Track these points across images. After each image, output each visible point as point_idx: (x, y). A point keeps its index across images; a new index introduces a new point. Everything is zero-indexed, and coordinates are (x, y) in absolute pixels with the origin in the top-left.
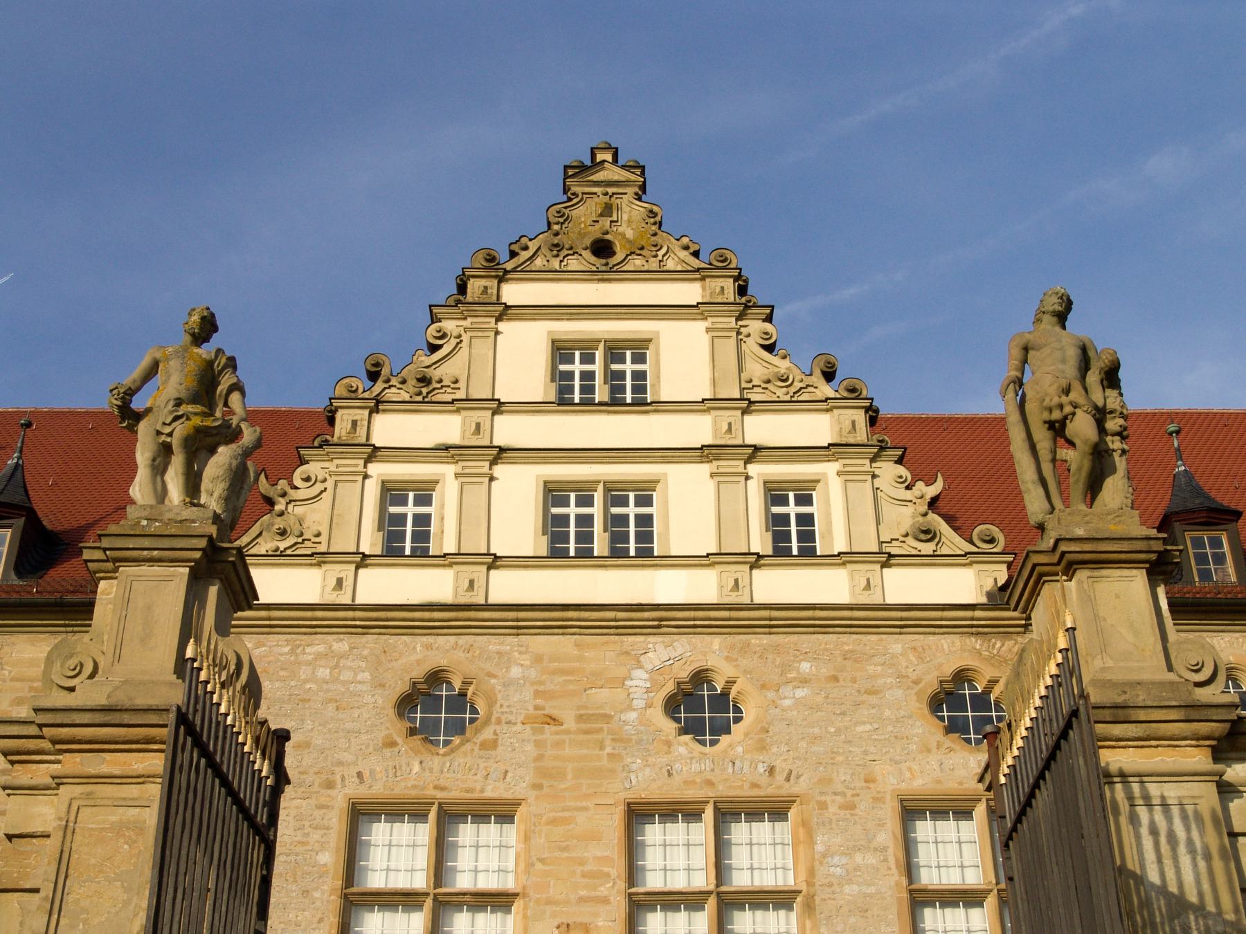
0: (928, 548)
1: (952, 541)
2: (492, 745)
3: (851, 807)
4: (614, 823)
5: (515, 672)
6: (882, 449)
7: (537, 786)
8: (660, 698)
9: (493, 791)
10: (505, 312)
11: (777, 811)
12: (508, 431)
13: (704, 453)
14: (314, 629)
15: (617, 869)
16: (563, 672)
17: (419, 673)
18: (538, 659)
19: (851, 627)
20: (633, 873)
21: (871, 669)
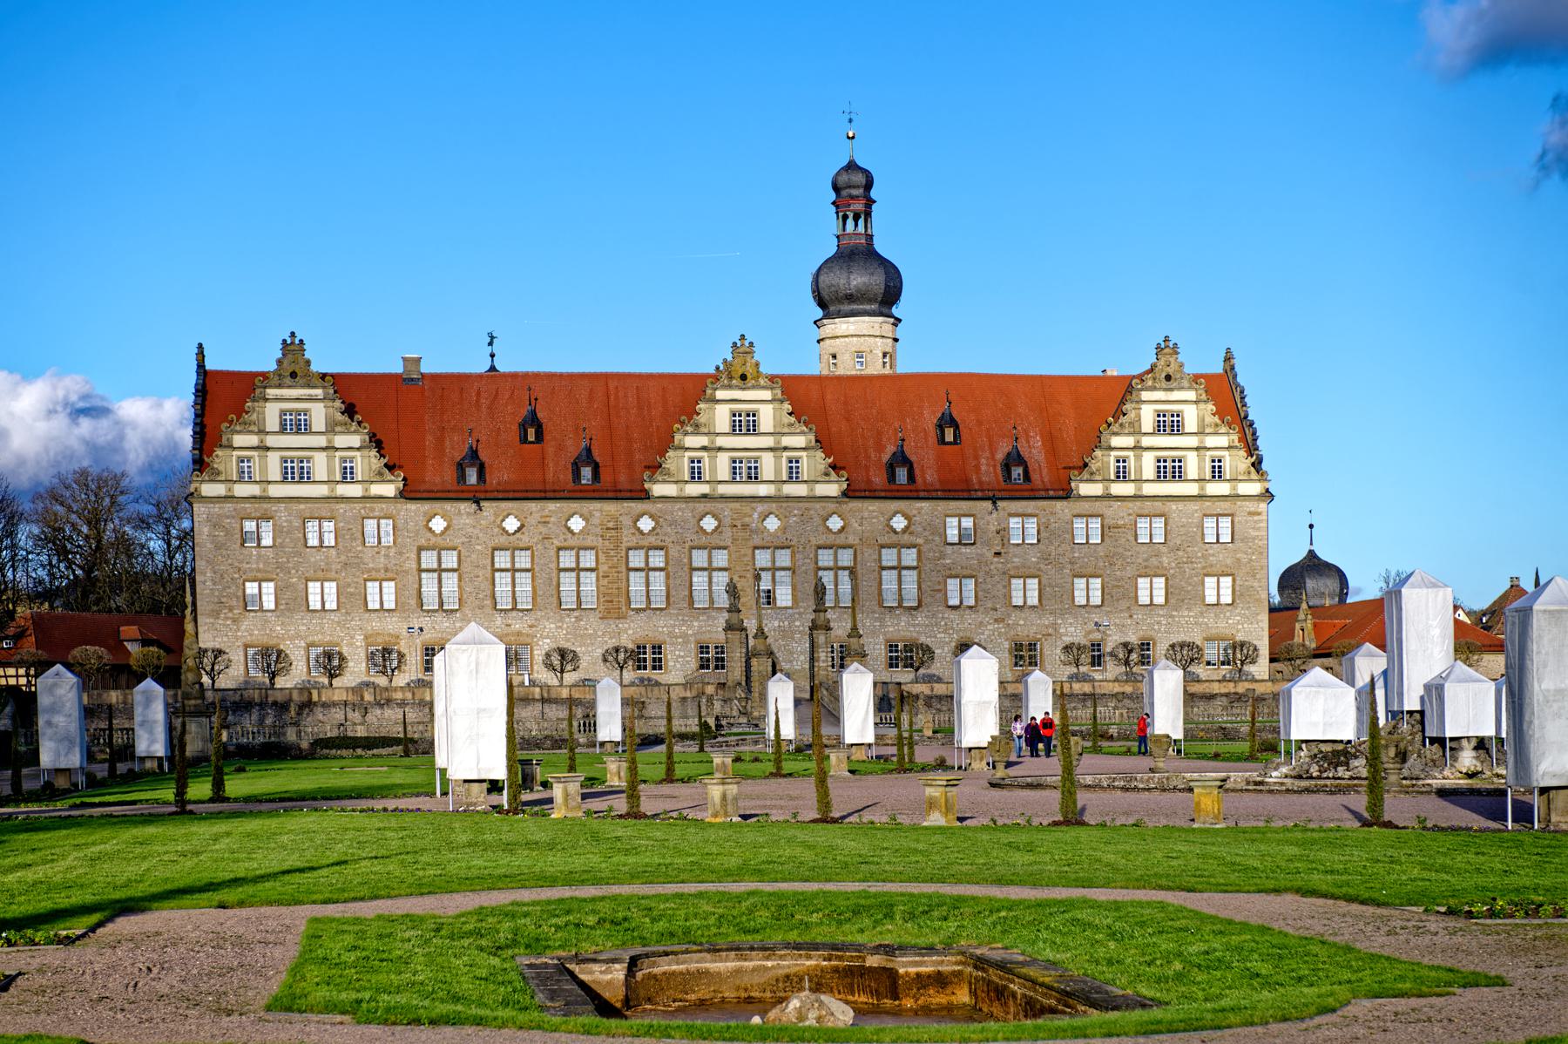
0: (827, 478)
1: (833, 476)
2: (721, 532)
9: (722, 544)
10: (718, 401)
11: (788, 548)
12: (721, 441)
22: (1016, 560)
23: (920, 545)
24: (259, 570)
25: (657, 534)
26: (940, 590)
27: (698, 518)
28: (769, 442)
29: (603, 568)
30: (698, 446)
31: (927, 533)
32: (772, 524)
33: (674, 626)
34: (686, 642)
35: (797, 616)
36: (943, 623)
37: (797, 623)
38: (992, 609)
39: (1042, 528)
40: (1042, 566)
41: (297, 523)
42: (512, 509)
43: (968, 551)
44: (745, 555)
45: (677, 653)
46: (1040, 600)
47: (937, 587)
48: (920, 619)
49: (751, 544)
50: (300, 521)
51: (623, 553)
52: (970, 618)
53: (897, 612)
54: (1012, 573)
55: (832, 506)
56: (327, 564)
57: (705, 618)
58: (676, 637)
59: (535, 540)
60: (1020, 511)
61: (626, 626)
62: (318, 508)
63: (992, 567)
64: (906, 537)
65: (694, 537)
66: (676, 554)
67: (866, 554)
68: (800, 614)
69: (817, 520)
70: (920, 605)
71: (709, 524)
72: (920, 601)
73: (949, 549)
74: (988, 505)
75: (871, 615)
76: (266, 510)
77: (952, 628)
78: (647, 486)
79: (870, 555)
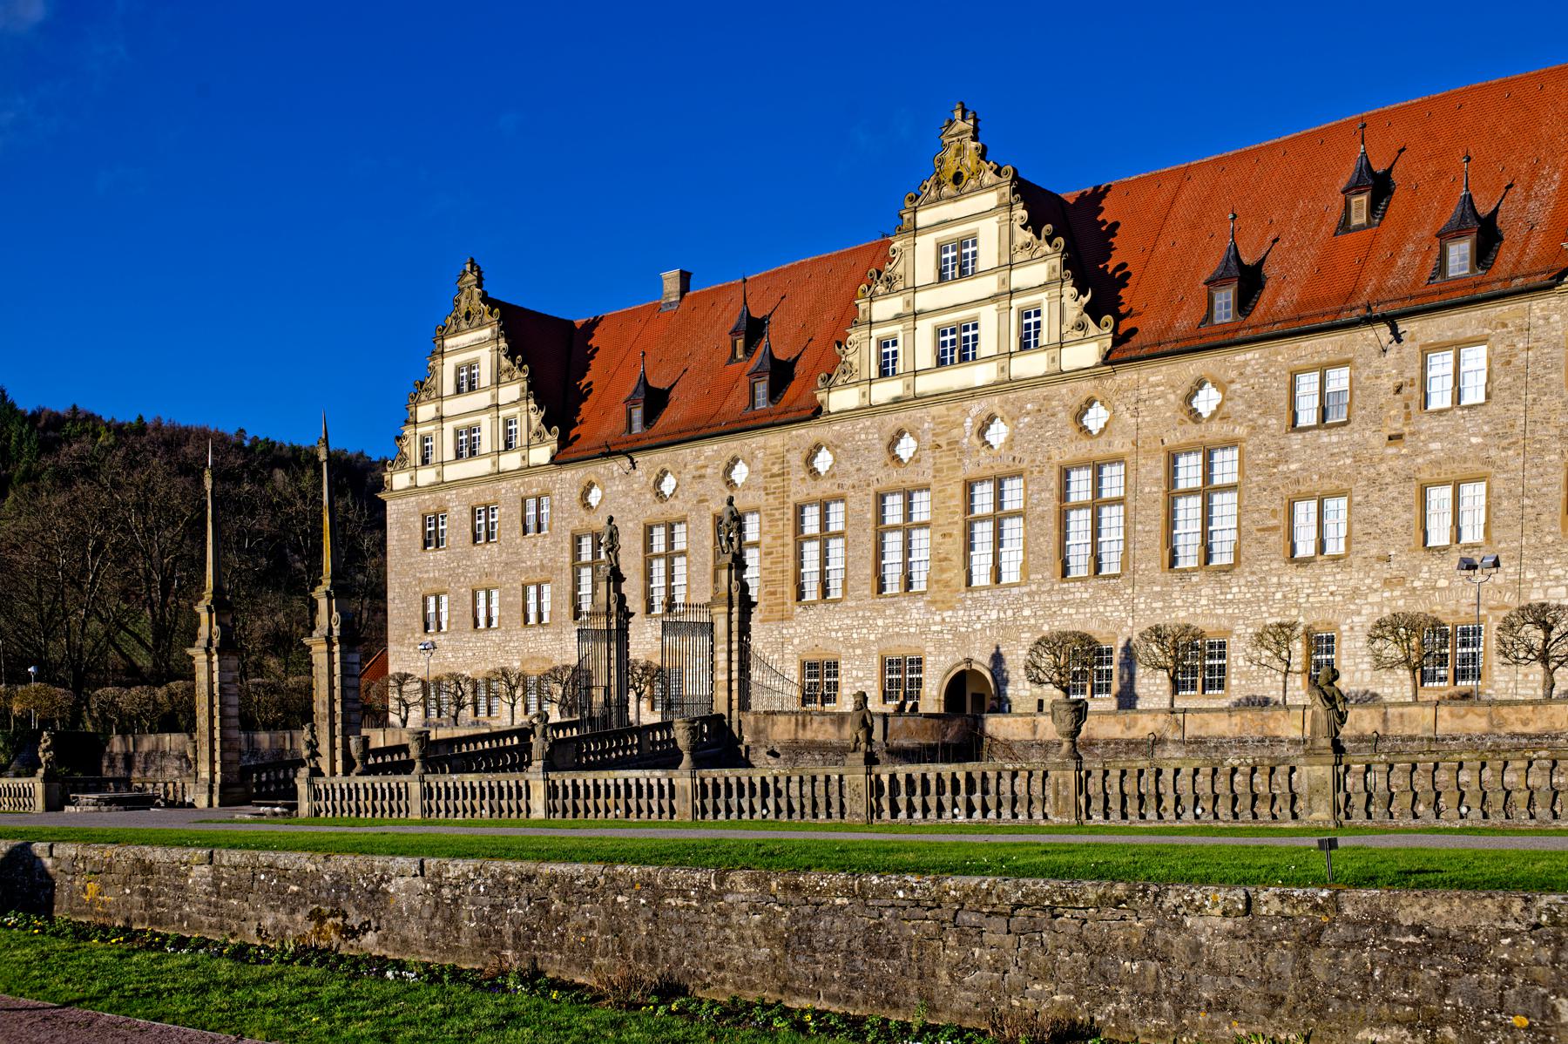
1: (1093, 329)
2: (918, 461)
3: (1041, 472)
4: (958, 490)
5: (926, 425)
6: (1063, 281)
7: (935, 477)
8: (975, 430)
9: (921, 480)
11: (1020, 475)
12: (924, 300)
13: (994, 298)
14: (858, 417)
15: (960, 510)
16: (941, 423)
17: (893, 432)
18: (934, 418)
19: (1045, 384)
20: (969, 509)
21: (1054, 403)
22: (1435, 446)
23: (1242, 440)
24: (435, 580)
25: (833, 476)
26: (1274, 529)
27: (888, 439)
28: (989, 285)
29: (767, 540)
30: (890, 315)
31: (1254, 414)
32: (998, 434)
33: (849, 628)
34: (867, 655)
35: (1026, 599)
36: (1279, 596)
37: (1027, 612)
38: (1379, 559)
39: (1496, 367)
40: (1493, 453)
41: (467, 515)
42: (665, 461)
43: (1335, 439)
44: (952, 496)
45: (854, 673)
46: (1486, 531)
47: (1272, 522)
48: (1237, 589)
49: (961, 475)
50: (469, 511)
51: (790, 513)
52: (1332, 579)
53: (1194, 579)
54: (1425, 476)
55: (1086, 387)
56: (492, 565)
57: (893, 612)
58: (854, 647)
59: (689, 506)
60: (1449, 335)
61: (791, 631)
62: (483, 491)
63: (1383, 468)
64: (1215, 427)
65: (881, 474)
66: (858, 508)
67: (1143, 470)
68: (1031, 594)
69: (1064, 417)
70: (1237, 562)
71: (906, 448)
72: (1237, 553)
73: (1297, 438)
74: (1384, 331)
75: (1147, 589)
76: (441, 500)
77: (1298, 606)
78: (821, 396)
79: (1150, 472)
